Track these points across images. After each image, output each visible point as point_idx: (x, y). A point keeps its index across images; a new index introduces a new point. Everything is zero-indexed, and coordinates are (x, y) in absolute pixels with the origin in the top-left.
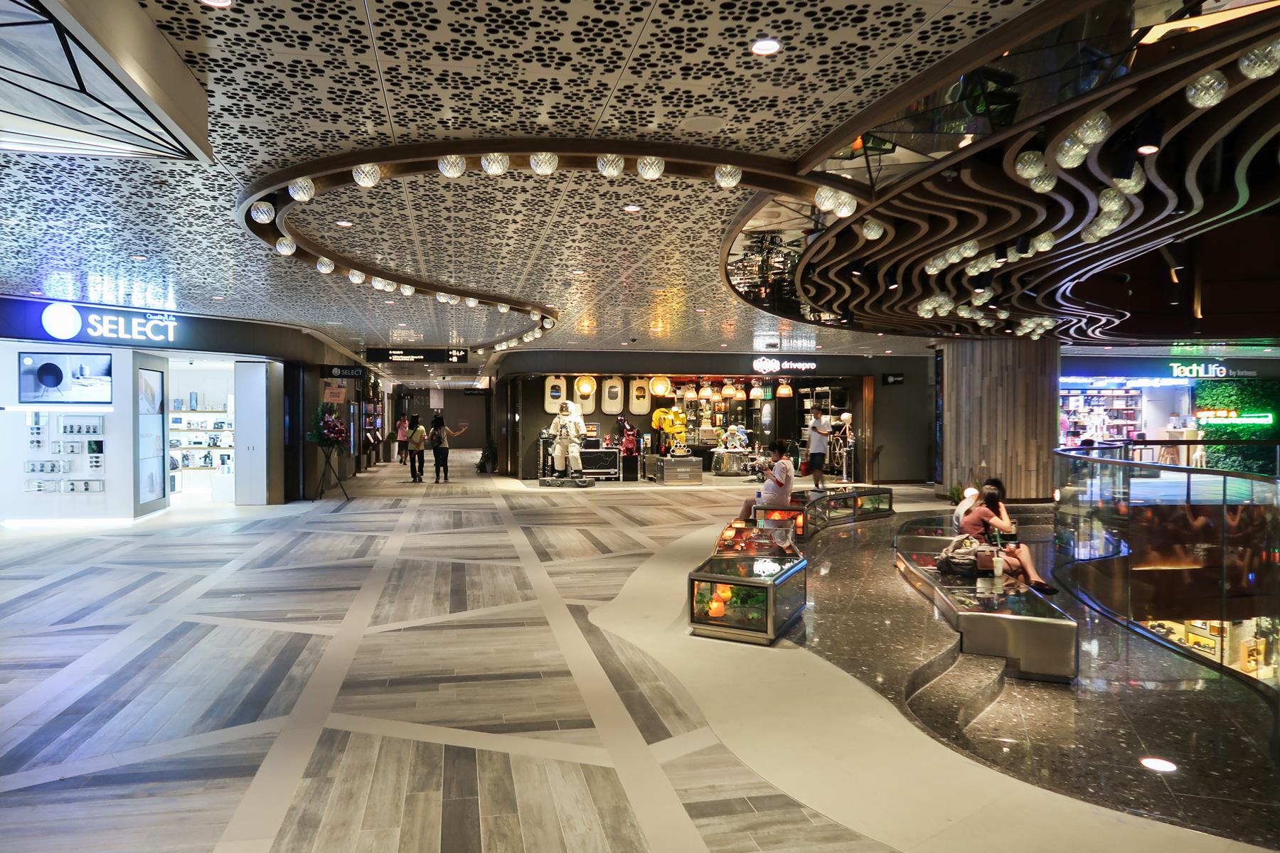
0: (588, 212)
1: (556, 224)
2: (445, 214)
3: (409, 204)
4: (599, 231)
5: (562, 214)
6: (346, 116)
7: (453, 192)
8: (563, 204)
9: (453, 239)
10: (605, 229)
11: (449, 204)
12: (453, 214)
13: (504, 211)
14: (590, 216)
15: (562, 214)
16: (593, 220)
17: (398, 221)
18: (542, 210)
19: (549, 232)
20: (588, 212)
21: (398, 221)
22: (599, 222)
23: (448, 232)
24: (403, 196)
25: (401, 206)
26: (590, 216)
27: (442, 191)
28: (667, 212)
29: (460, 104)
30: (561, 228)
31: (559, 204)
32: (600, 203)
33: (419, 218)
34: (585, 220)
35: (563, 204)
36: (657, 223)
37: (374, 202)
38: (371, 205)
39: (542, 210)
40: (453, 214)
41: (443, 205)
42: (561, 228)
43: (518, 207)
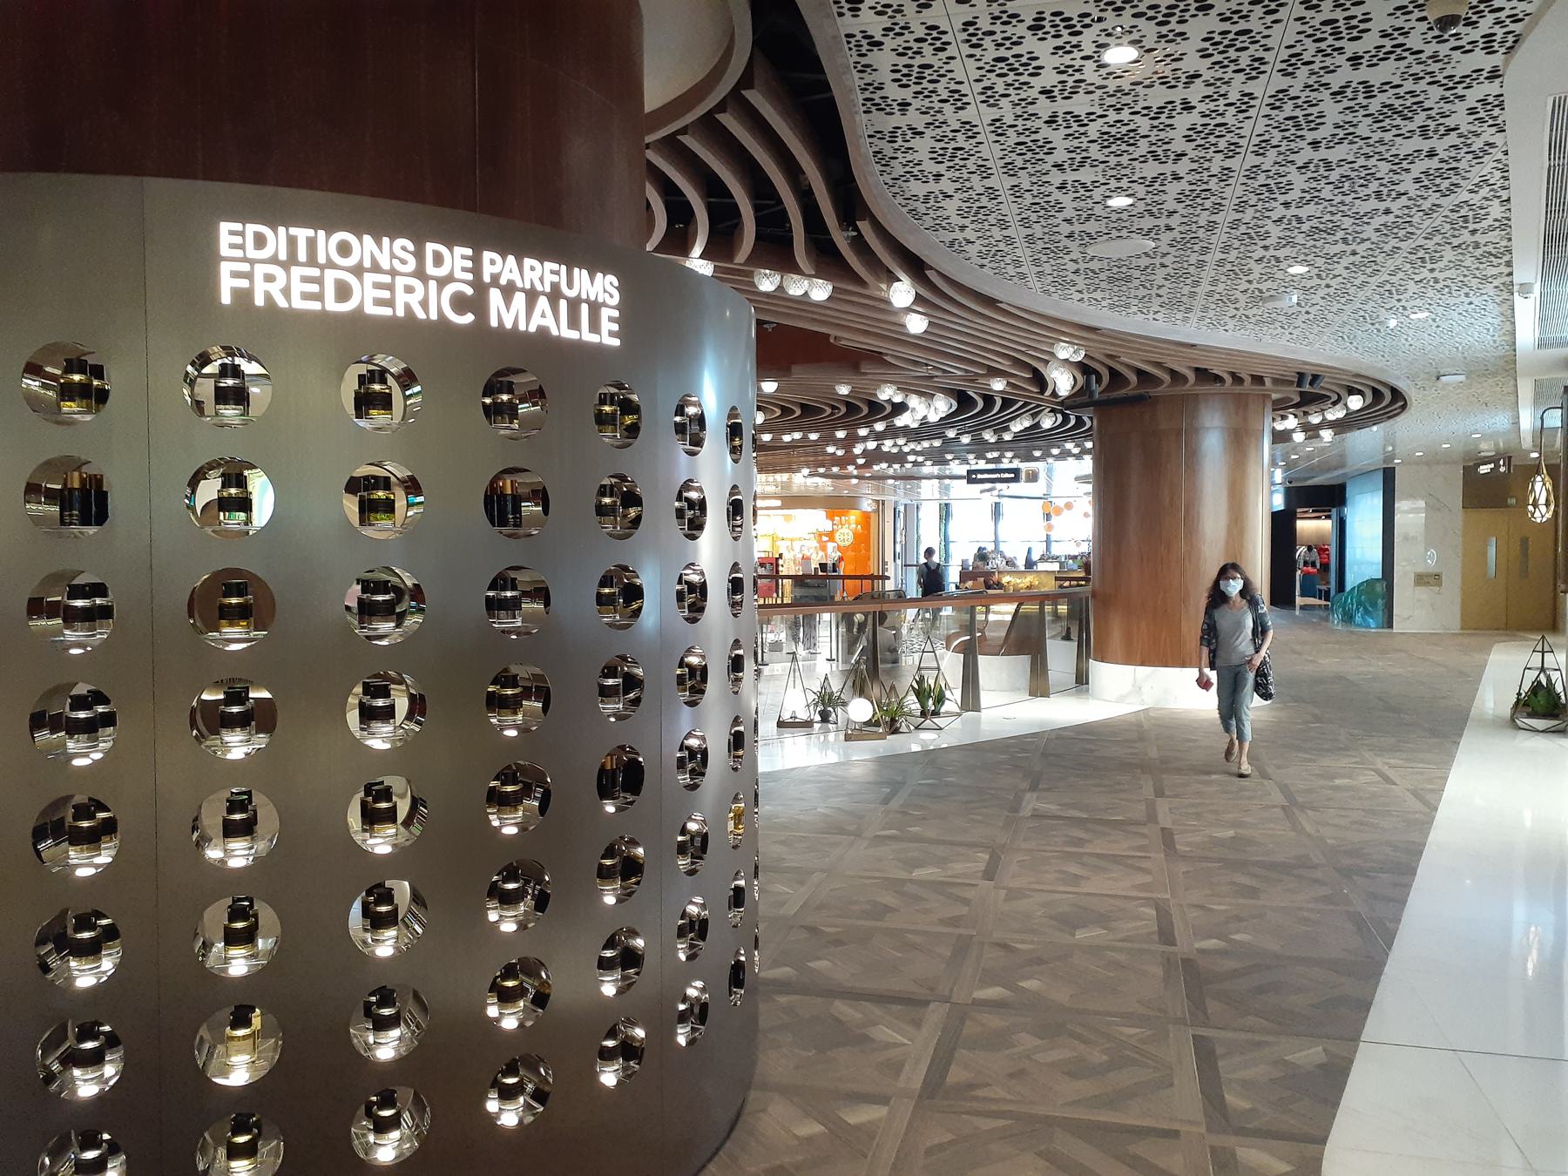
0: (1282, 199)
1: (1234, 225)
2: (1065, 229)
3: (1013, 220)
4: (1305, 227)
5: (1241, 206)
6: (916, 103)
7: (1072, 195)
8: (1239, 191)
9: (1082, 266)
10: (1315, 223)
11: (1069, 213)
12: (1077, 228)
13: (1151, 214)
14: (1286, 205)
15: (1241, 206)
16: (1293, 211)
17: (1002, 246)
18: (1208, 204)
19: (1224, 238)
20: (1282, 199)
21: (1002, 246)
22: (1303, 213)
23: (1073, 256)
24: (1004, 209)
25: (1003, 224)
26: (1286, 205)
27: (1057, 195)
28: (1417, 180)
29: (1076, 143)
30: (1243, 229)
31: (1233, 192)
32: (1299, 181)
33: (1030, 239)
34: (1280, 211)
35: (1239, 191)
36: (1403, 200)
37: (966, 222)
38: (963, 228)
39: (1208, 204)
40: (1077, 228)
41: (1061, 216)
42: (1243, 229)
43: (1171, 205)
